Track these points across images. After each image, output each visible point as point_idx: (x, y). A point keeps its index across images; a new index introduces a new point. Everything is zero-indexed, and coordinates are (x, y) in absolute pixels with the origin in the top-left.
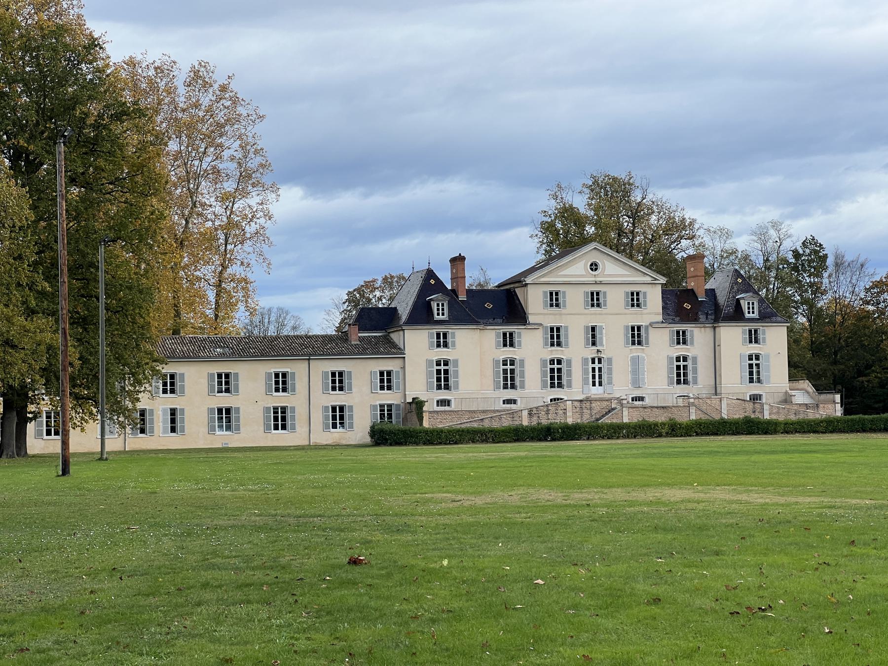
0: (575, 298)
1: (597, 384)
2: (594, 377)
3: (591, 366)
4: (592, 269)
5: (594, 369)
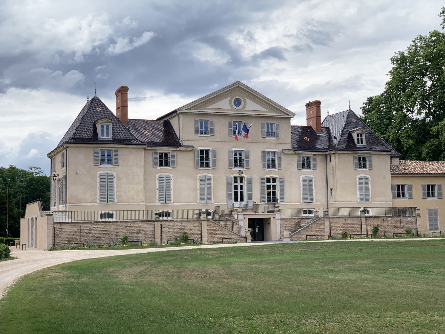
0: (221, 128)
1: (239, 199)
2: (236, 193)
3: (233, 184)
4: (235, 105)
5: (236, 187)
